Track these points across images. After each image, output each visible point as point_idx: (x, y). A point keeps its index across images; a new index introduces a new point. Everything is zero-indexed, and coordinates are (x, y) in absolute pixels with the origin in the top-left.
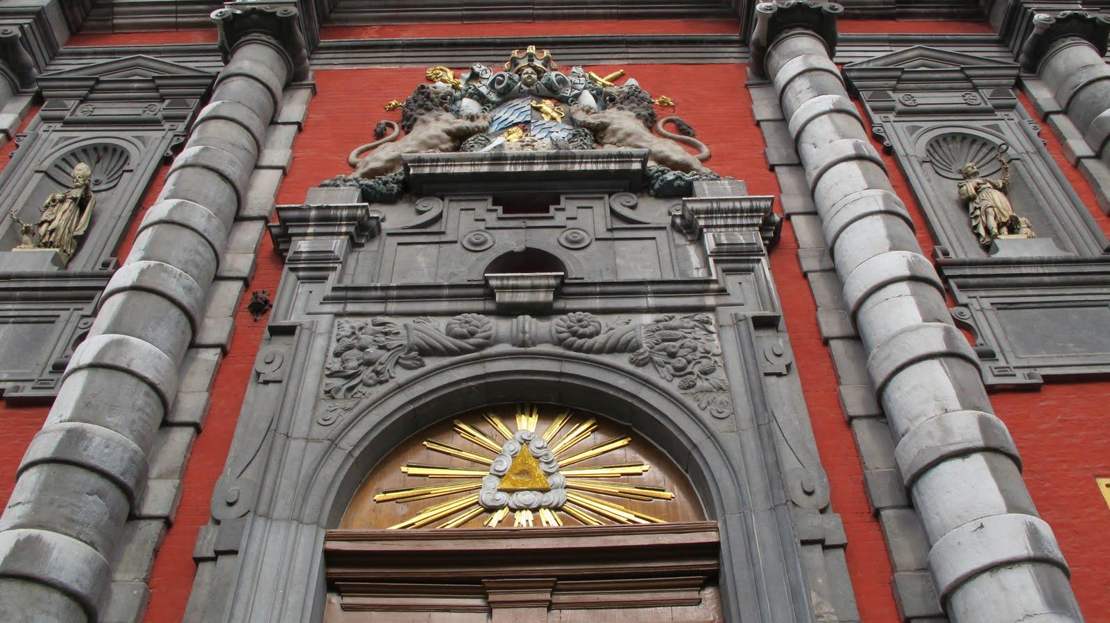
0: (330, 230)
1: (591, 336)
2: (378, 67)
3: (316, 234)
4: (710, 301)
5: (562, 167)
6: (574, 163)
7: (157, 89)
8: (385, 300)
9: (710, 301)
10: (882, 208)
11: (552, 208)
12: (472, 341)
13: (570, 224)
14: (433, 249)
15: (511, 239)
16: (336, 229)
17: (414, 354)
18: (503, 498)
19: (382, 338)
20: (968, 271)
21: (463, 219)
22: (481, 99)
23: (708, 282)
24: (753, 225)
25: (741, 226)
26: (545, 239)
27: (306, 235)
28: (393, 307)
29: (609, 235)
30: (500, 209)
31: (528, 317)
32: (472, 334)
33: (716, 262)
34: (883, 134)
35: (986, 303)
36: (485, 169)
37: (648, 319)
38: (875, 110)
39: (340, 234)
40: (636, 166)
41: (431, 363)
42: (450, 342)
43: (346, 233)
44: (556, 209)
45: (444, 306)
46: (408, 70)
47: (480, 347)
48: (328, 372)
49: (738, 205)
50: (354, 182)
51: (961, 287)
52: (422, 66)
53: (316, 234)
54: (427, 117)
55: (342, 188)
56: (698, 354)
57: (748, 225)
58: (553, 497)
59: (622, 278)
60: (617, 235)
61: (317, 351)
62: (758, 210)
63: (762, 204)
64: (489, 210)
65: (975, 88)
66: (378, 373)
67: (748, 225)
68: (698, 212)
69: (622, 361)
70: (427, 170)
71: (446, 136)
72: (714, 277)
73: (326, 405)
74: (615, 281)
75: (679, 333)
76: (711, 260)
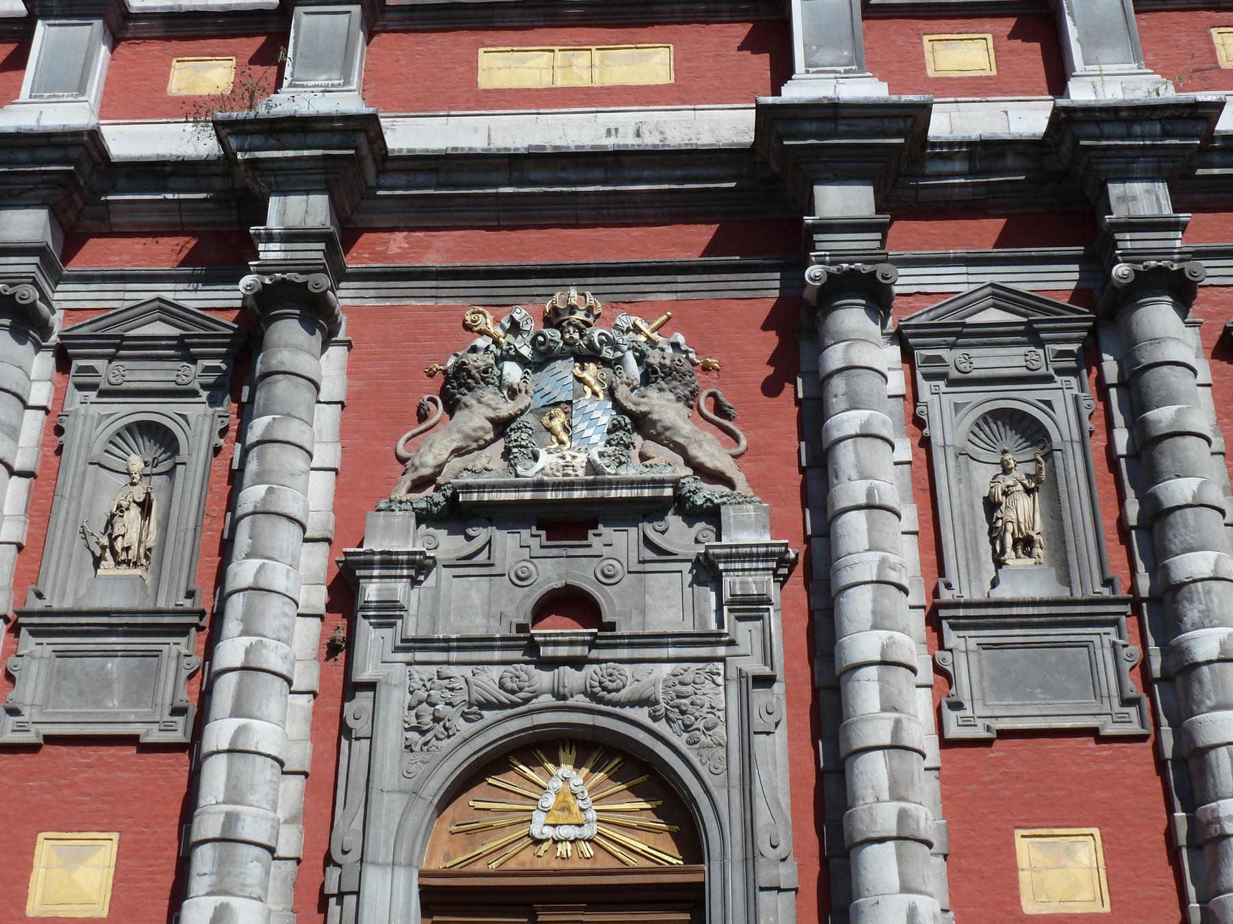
0: (393, 572)
1: (617, 690)
2: (413, 302)
3: (381, 577)
5: (599, 494)
6: (610, 489)
8: (448, 650)
9: (721, 651)
10: (875, 579)
11: (590, 532)
12: (521, 695)
13: (606, 551)
14: (484, 582)
15: (552, 570)
16: (398, 572)
17: (475, 709)
18: (549, 832)
19: (448, 694)
20: (961, 612)
21: (511, 546)
23: (720, 635)
24: (768, 569)
25: (757, 569)
27: (371, 577)
28: (454, 656)
29: (640, 567)
30: (543, 533)
31: (567, 668)
32: (521, 689)
33: (730, 611)
34: (925, 418)
35: (972, 643)
36: (528, 496)
37: (668, 668)
38: (927, 377)
39: (402, 577)
40: (668, 492)
42: (504, 697)
43: (408, 577)
44: (595, 535)
45: (497, 655)
46: (446, 308)
47: (526, 701)
48: (407, 726)
49: (754, 550)
50: (408, 506)
51: (954, 627)
52: (459, 302)
53: (381, 577)
54: (468, 399)
55: (398, 513)
56: (705, 709)
57: (763, 569)
58: (589, 831)
59: (647, 632)
60: (648, 567)
61: (394, 708)
62: (773, 554)
63: (777, 549)
64: (532, 536)
65: (1040, 344)
66: (447, 729)
67: (763, 569)
68: (718, 556)
69: (641, 714)
70: (475, 497)
71: (489, 425)
72: (725, 631)
74: (641, 632)
75: (689, 689)
76: (725, 608)
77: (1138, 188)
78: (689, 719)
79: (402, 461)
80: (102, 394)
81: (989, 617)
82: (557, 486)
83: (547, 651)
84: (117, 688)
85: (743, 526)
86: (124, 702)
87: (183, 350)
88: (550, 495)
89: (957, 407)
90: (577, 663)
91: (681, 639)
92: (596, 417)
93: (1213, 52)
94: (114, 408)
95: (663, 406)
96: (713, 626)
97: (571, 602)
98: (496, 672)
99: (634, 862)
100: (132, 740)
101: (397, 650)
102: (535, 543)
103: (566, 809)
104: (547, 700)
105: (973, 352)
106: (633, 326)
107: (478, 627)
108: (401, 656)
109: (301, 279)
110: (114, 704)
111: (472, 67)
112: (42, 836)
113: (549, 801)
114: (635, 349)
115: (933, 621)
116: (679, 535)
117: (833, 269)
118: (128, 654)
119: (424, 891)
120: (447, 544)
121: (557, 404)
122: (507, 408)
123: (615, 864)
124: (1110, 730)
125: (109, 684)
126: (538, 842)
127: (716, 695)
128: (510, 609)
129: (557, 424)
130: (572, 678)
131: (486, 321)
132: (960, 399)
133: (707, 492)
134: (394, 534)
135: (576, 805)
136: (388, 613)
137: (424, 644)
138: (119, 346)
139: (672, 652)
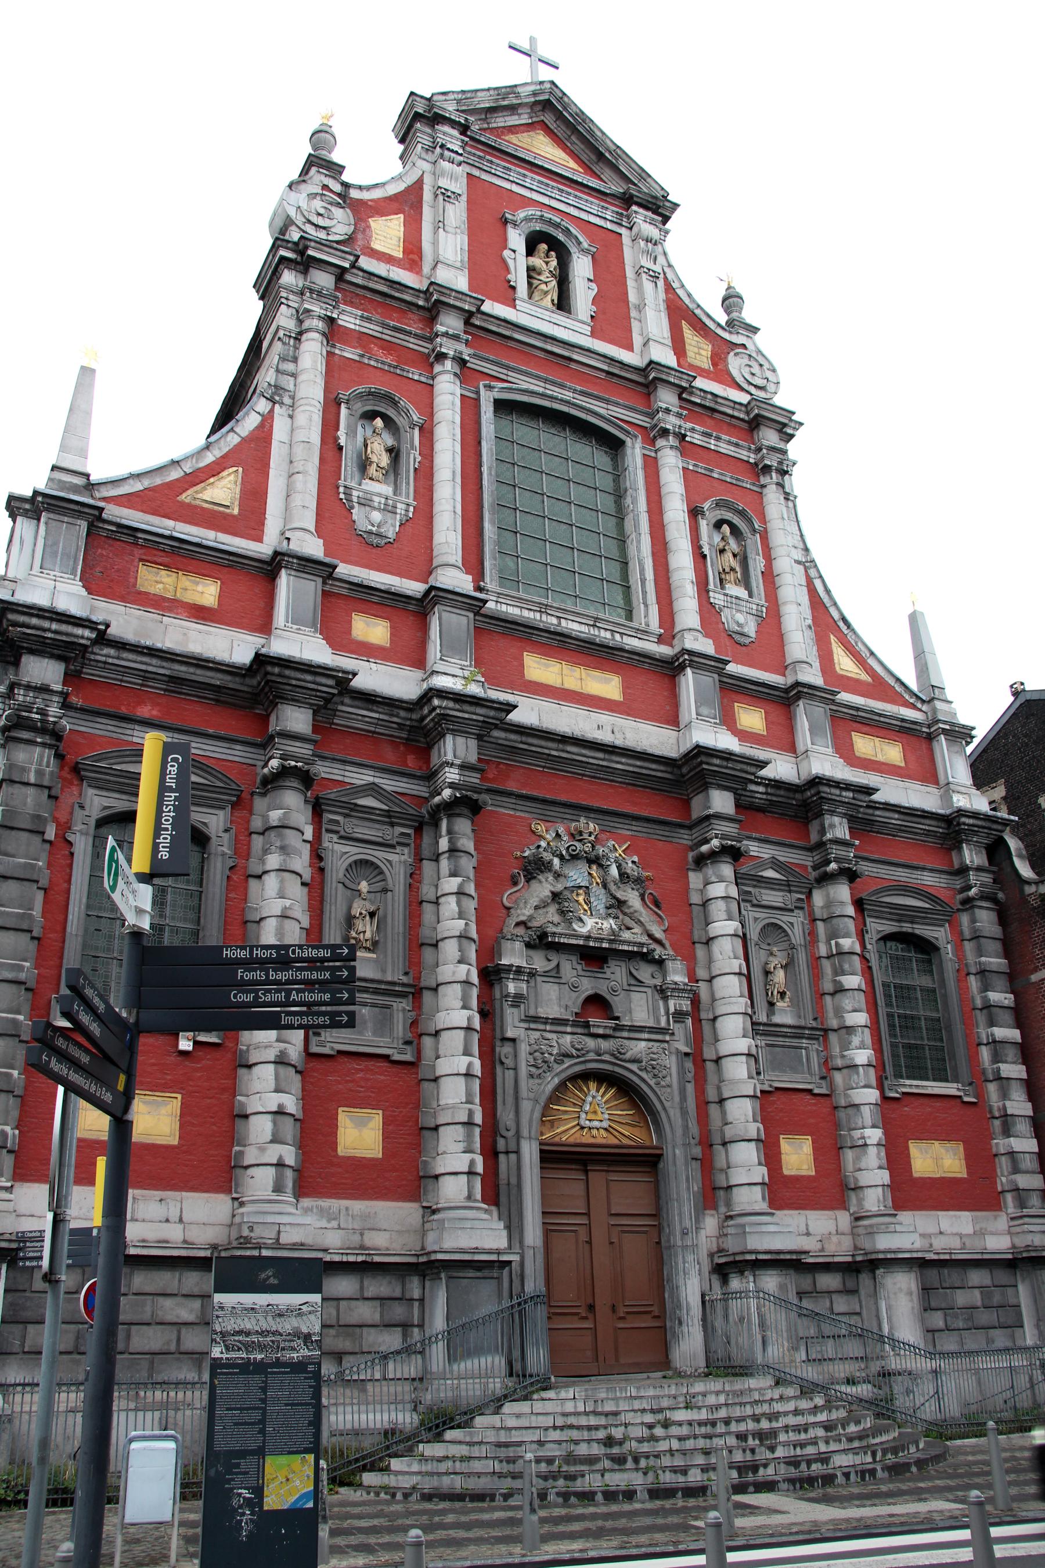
4: (667, 1038)
5: (614, 946)
7: (390, 817)
14: (556, 987)
15: (588, 987)
22: (561, 857)
26: (602, 988)
28: (548, 1027)
36: (581, 942)
37: (643, 1044)
41: (568, 1062)
45: (569, 1029)
52: (526, 815)
58: (605, 1124)
65: (790, 891)
69: (634, 1067)
73: (531, 1081)
77: (836, 820)
78: (656, 1071)
79: (508, 909)
80: (341, 837)
82: (596, 939)
83: (593, 1030)
84: (370, 1025)
85: (675, 972)
86: (374, 1034)
87: (390, 818)
88: (591, 944)
89: (756, 919)
90: (604, 1037)
91: (652, 1030)
92: (600, 900)
93: (852, 745)
94: (347, 849)
95: (632, 897)
96: (663, 1024)
98: (568, 1038)
99: (626, 1141)
100: (386, 1057)
101: (522, 1021)
102: (579, 967)
103: (595, 1112)
104: (592, 1056)
105: (763, 891)
108: (523, 1025)
109: (475, 796)
110: (369, 1035)
112: (340, 1109)
113: (587, 1108)
114: (616, 862)
116: (645, 972)
117: (724, 842)
118: (374, 1005)
119: (541, 1151)
120: (539, 962)
121: (580, 887)
122: (559, 887)
123: (616, 1142)
124: (816, 1091)
125: (365, 1022)
126: (583, 1128)
128: (570, 1003)
129: (581, 899)
130: (604, 1045)
131: (540, 828)
132: (758, 915)
135: (599, 1110)
137: (536, 1019)
138: (352, 810)
139: (646, 1036)
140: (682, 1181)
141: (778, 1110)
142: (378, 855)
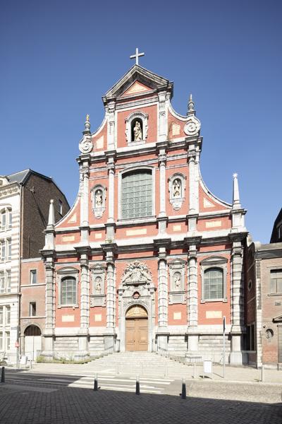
15: (135, 290)
61: (122, 303)
81: (174, 293)
92: (139, 274)
95: (145, 273)
97: (137, 293)
106: (142, 263)
107: (129, 295)
111: (125, 233)
115: (169, 293)
120: (126, 288)
127: (150, 301)
133: (148, 282)
134: (121, 287)
136: (121, 295)
140: (151, 321)
141: (173, 307)
142: (100, 275)
